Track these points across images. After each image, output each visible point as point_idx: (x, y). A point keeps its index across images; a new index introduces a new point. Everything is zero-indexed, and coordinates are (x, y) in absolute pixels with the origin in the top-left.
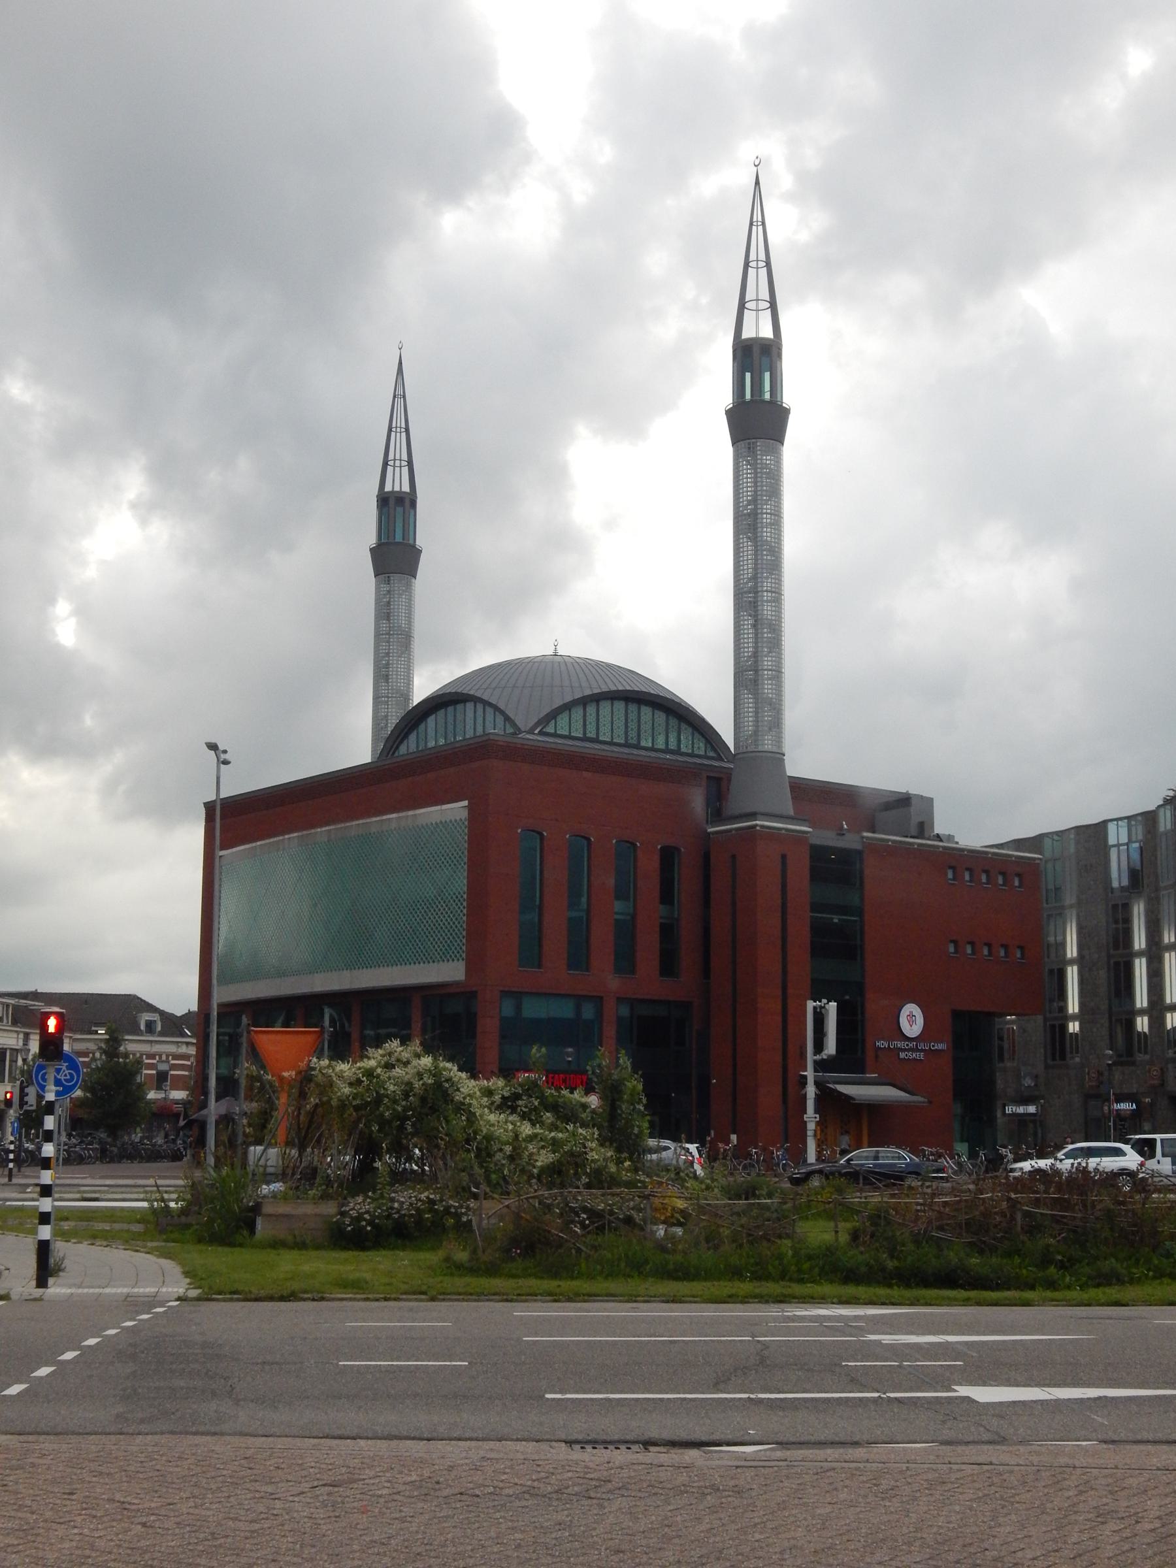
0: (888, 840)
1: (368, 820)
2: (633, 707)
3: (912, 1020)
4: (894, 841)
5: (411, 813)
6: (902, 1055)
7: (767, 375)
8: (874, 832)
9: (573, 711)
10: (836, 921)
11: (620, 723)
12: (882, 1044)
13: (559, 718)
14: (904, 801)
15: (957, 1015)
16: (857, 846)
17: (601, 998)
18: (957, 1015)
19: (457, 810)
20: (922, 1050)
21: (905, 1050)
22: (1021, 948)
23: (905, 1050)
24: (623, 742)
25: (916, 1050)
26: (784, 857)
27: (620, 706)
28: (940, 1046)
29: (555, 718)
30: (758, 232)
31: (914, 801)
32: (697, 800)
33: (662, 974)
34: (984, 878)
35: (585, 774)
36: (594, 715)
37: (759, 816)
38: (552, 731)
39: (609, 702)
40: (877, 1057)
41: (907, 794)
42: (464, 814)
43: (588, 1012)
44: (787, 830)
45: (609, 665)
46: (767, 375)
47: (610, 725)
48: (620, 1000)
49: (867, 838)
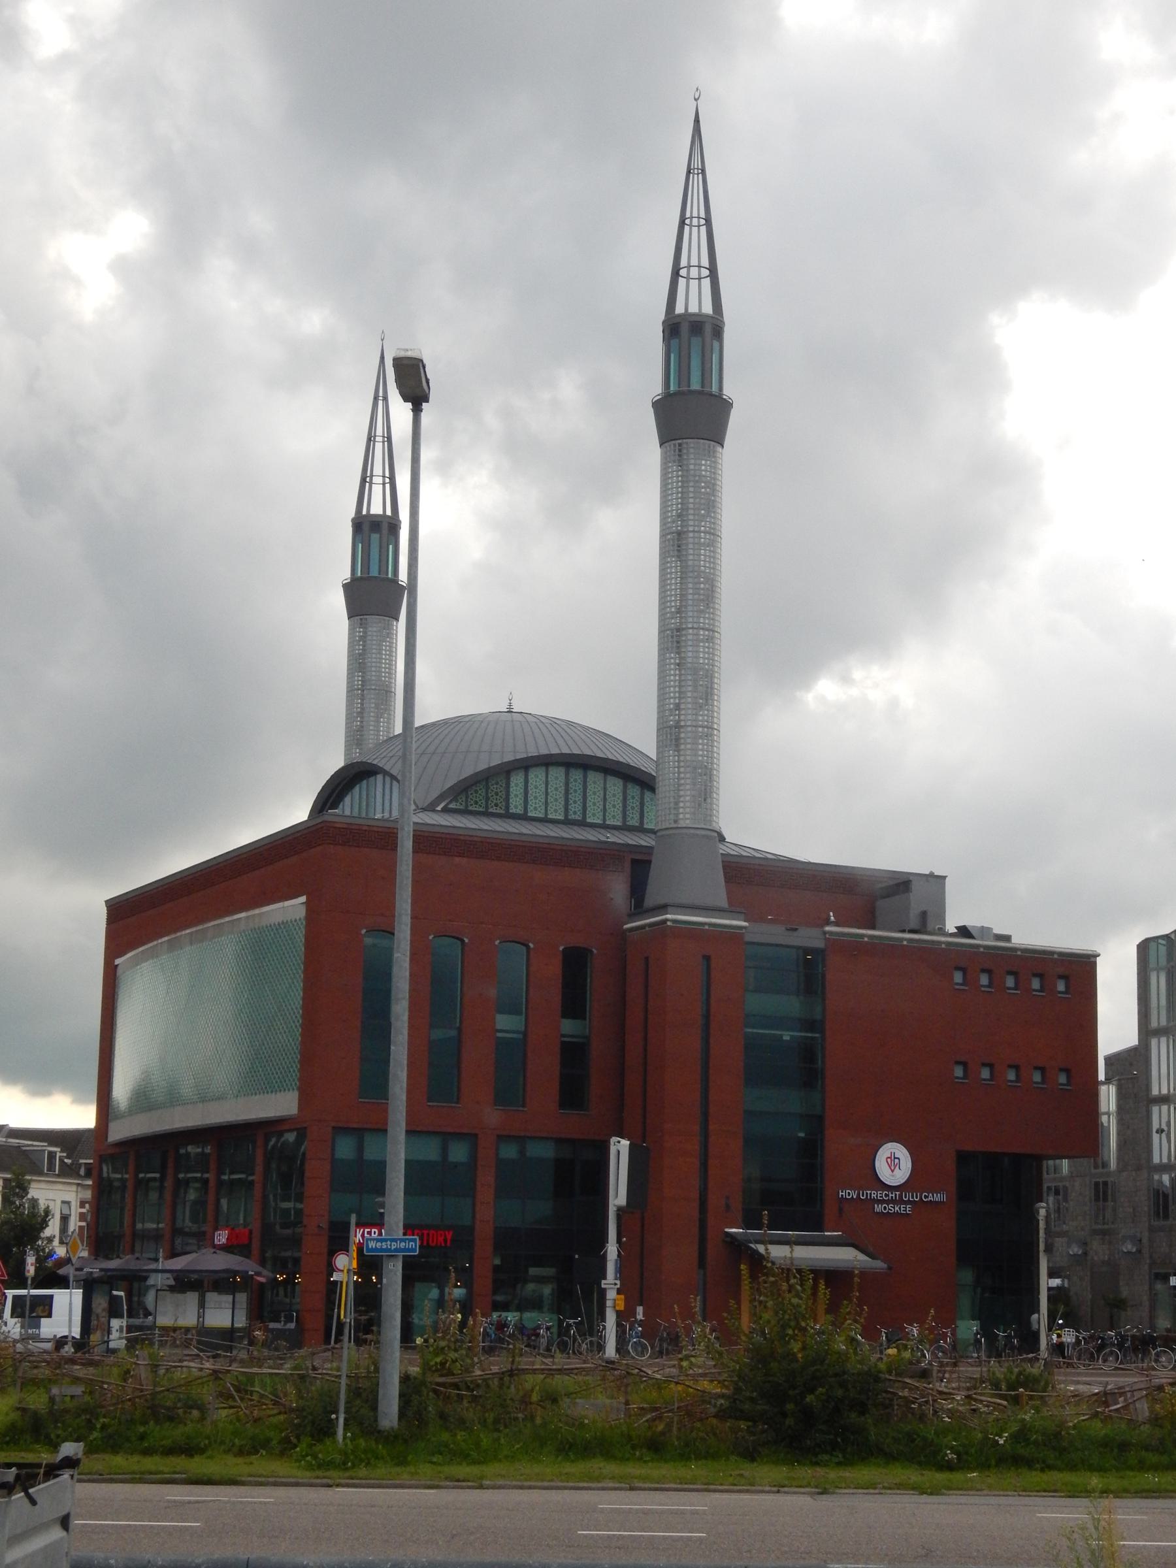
0: (863, 936)
1: (222, 921)
2: (576, 775)
3: (894, 1164)
5: (257, 911)
6: (878, 1208)
8: (873, 928)
9: (532, 774)
11: (557, 794)
12: (849, 1194)
14: (901, 884)
15: (963, 1158)
16: (819, 944)
17: (476, 1135)
18: (963, 1158)
19: (294, 908)
20: (909, 1202)
22: (1067, 1071)
24: (561, 817)
25: (901, 1201)
26: (707, 958)
27: (557, 774)
28: (937, 1197)
31: (915, 886)
32: (617, 889)
33: (562, 1105)
34: (1010, 982)
35: (457, 860)
36: (521, 785)
37: (670, 909)
39: (544, 768)
40: (841, 1210)
42: (302, 913)
43: (459, 1153)
44: (710, 925)
45: (554, 721)
47: (541, 794)
48: (502, 1138)
49: (831, 933)
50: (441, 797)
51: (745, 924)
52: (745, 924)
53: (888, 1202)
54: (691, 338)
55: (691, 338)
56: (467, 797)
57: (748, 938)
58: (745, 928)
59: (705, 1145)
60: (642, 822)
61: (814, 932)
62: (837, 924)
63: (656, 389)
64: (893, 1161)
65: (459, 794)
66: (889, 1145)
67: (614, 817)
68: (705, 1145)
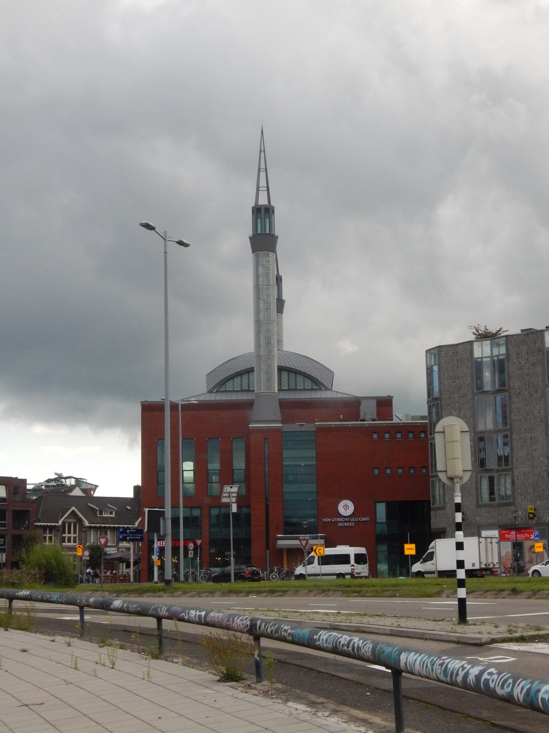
0: (332, 425)
4: (334, 425)
6: (340, 524)
7: (267, 220)
13: (227, 383)
20: (352, 522)
21: (341, 522)
23: (341, 522)
25: (350, 521)
28: (366, 519)
29: (225, 383)
41: (389, 396)
44: (267, 427)
46: (267, 220)
50: (214, 387)
54: (263, 213)
55: (263, 213)
57: (283, 430)
59: (267, 506)
60: (296, 387)
61: (310, 425)
62: (344, 420)
63: (250, 233)
64: (346, 507)
65: (223, 385)
68: (267, 506)
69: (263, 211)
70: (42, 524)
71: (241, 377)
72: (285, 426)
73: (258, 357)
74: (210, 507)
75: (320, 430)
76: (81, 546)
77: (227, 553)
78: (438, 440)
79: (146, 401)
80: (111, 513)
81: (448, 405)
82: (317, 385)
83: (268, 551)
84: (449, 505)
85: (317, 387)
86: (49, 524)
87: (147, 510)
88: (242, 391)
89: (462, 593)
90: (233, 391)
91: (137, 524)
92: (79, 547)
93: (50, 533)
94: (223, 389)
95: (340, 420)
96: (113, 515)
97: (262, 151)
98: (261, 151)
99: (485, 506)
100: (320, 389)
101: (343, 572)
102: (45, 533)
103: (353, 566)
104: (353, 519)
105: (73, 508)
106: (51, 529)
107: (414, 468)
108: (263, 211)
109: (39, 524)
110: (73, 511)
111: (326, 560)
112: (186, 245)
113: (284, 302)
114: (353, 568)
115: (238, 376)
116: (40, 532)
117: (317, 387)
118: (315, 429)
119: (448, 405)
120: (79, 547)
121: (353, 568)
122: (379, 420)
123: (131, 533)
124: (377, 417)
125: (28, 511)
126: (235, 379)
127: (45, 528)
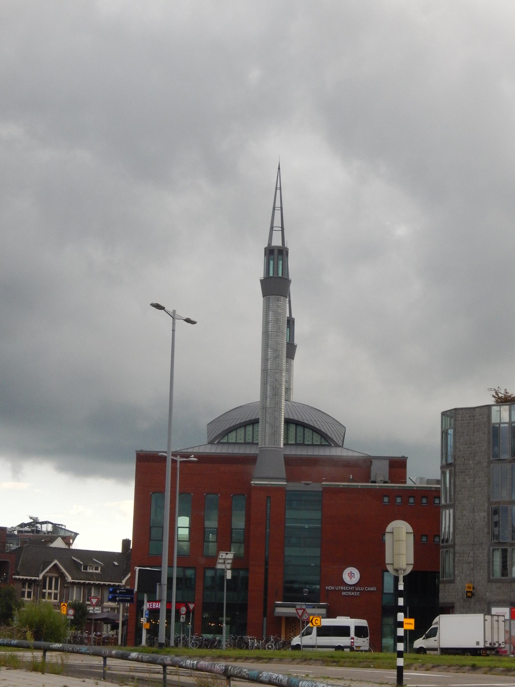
6: (344, 593)
7: (280, 262)
10: (306, 527)
13: (229, 435)
17: (195, 567)
20: (358, 591)
25: (354, 591)
28: (372, 589)
30: (278, 191)
38: (226, 441)
41: (403, 457)
44: (270, 484)
46: (280, 262)
51: (286, 483)
52: (286, 483)
53: (349, 591)
54: (276, 255)
55: (276, 255)
56: (228, 437)
57: (288, 489)
58: (286, 485)
59: (266, 570)
62: (354, 481)
63: (261, 275)
64: (351, 575)
65: (225, 436)
66: (349, 568)
67: (308, 441)
68: (266, 570)
69: (276, 252)
70: (21, 577)
71: (245, 428)
72: (291, 484)
73: (264, 408)
74: (205, 568)
75: (327, 490)
76: (66, 604)
77: (220, 619)
78: (388, 538)
79: (141, 451)
80: (96, 569)
81: (462, 472)
82: (326, 440)
83: (265, 619)
84: (459, 578)
85: (327, 443)
86: (29, 578)
87: (137, 569)
88: (246, 443)
89: (400, 662)
90: (236, 443)
91: (124, 582)
92: (64, 605)
93: (29, 587)
94: (225, 440)
95: (349, 481)
96: (99, 571)
97: (278, 188)
98: (276, 188)
99: (497, 581)
100: (329, 445)
101: (342, 645)
102: (24, 587)
103: (352, 638)
104: (358, 589)
105: (56, 561)
106: (31, 583)
107: (426, 536)
108: (276, 252)
109: (18, 577)
110: (56, 565)
111: (323, 631)
112: (193, 323)
113: (296, 346)
114: (352, 641)
115: (240, 427)
116: (17, 586)
117: (327, 443)
118: (321, 489)
119: (462, 472)
120: (64, 605)
121: (352, 641)
122: (391, 483)
123: (121, 593)
124: (390, 478)
125: (6, 562)
126: (239, 431)
127: (24, 582)
